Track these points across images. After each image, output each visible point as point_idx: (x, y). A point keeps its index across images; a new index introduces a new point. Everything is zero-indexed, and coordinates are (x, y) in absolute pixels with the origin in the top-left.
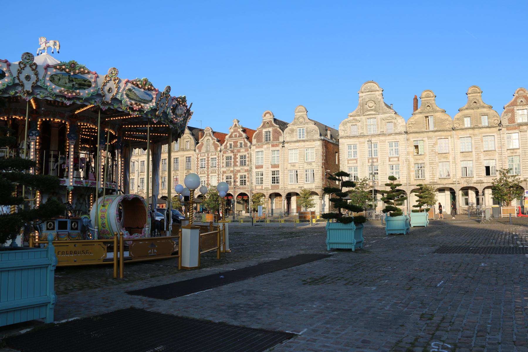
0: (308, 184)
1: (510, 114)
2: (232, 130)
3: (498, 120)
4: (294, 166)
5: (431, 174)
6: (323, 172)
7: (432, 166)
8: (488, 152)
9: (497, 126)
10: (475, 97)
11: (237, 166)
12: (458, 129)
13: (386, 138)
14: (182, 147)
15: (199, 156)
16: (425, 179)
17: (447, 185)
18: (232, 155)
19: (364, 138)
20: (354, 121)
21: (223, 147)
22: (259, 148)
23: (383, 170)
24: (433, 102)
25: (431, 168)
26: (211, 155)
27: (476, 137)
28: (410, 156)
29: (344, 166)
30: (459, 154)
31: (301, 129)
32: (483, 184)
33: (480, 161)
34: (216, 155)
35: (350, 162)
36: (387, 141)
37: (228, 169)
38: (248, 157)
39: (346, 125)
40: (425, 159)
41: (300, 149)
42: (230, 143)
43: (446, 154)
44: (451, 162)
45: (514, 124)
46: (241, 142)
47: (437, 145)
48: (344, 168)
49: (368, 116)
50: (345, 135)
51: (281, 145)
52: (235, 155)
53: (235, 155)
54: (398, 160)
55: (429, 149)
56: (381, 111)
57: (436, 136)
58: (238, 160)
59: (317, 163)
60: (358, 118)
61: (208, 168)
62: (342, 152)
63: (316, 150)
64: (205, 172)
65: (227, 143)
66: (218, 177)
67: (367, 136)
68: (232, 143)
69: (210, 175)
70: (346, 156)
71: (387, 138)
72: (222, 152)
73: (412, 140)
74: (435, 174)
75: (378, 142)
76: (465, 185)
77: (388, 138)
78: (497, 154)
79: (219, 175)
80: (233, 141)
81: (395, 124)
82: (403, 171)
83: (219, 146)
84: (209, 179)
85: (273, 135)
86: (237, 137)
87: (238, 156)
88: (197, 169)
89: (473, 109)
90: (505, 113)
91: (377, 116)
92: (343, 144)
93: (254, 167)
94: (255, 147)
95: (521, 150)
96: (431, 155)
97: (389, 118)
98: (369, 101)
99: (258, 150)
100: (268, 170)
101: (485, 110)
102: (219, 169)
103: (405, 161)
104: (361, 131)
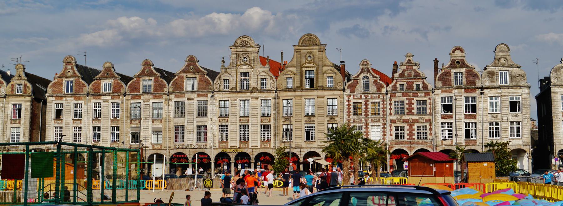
0: (519, 139)
2: (404, 67)
4: (496, 117)
11: (413, 114)
14: (320, 85)
15: (351, 98)
18: (404, 99)
21: (390, 88)
22: (445, 92)
26: (371, 98)
31: (503, 72)
34: (379, 98)
37: (399, 117)
38: (430, 104)
39: (559, 72)
41: (504, 97)
42: (402, 83)
46: (418, 83)
48: (558, 122)
50: (558, 83)
51: (479, 91)
52: (410, 100)
53: (410, 100)
58: (415, 106)
61: (366, 115)
62: (555, 103)
64: (361, 120)
65: (396, 83)
66: (384, 128)
68: (405, 83)
69: (370, 124)
72: (389, 95)
79: (384, 124)
80: (407, 81)
83: (383, 87)
84: (368, 130)
85: (466, 77)
86: (411, 77)
87: (414, 101)
88: (349, 115)
92: (556, 93)
93: (440, 117)
94: (440, 91)
99: (444, 95)
100: (460, 121)
102: (384, 117)
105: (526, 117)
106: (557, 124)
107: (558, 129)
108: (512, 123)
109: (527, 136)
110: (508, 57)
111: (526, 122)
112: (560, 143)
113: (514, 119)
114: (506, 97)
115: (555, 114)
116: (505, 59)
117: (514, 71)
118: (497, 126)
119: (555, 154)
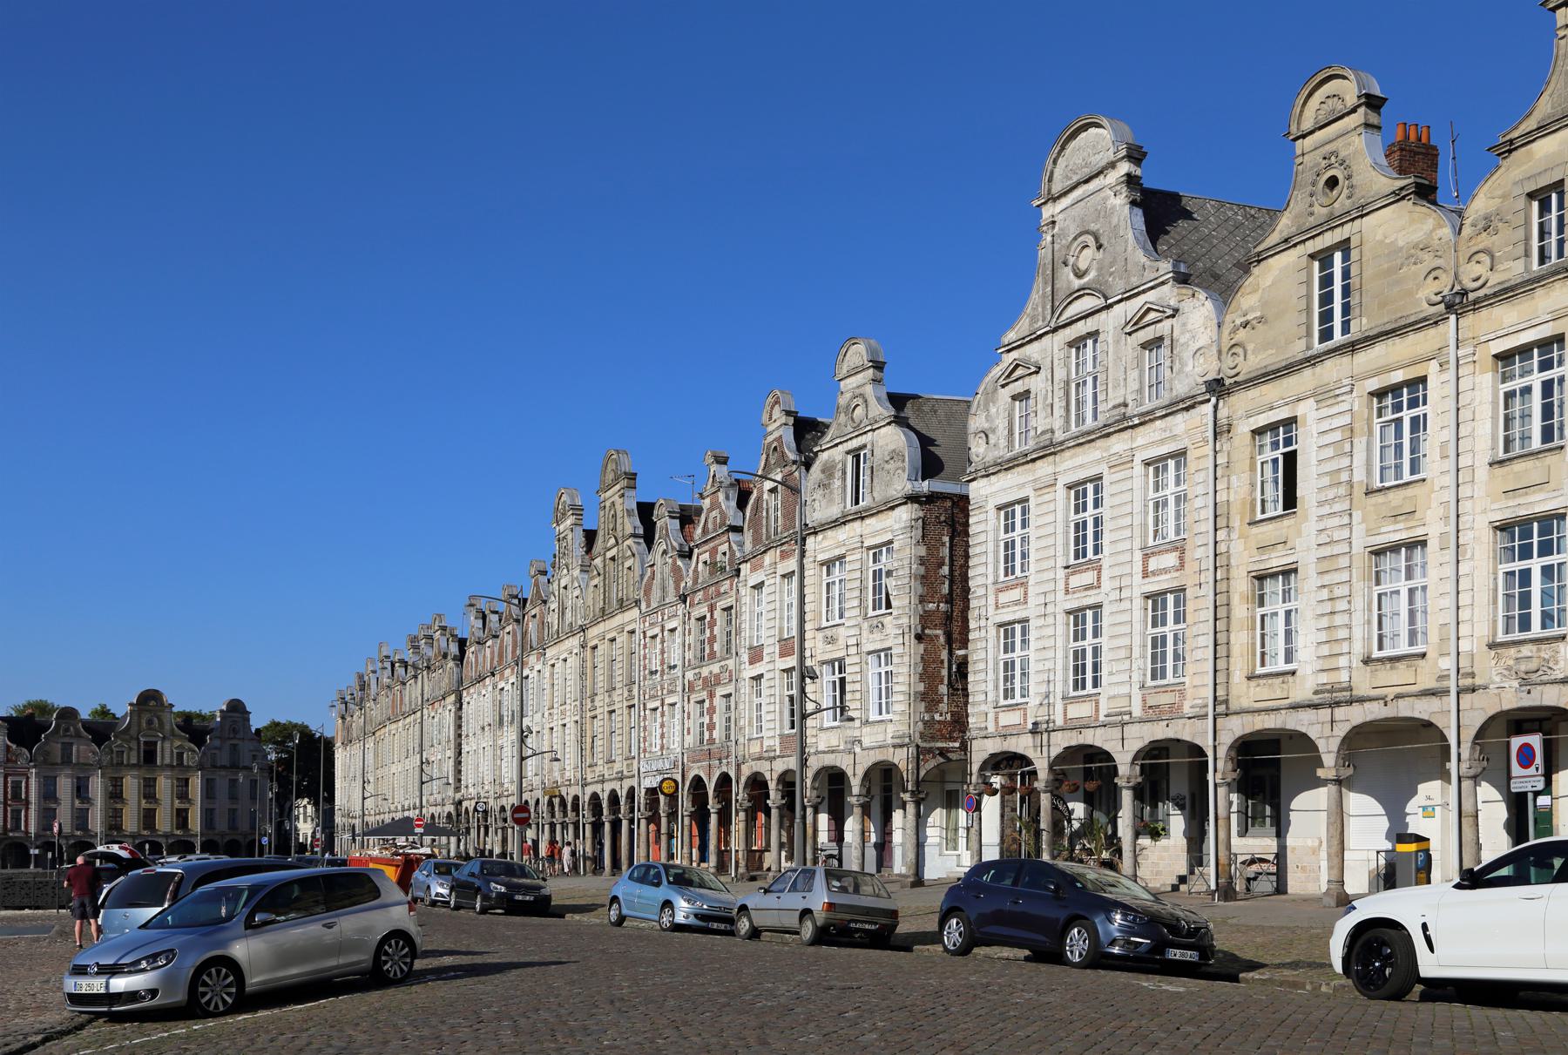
19: (1051, 458)
25: (1325, 594)
28: (1234, 536)
30: (1482, 472)
40: (1298, 543)
43: (1409, 491)
44: (1433, 544)
71: (1140, 441)
73: (1243, 428)
74: (1342, 633)
77: (1144, 436)
97: (1152, 316)
112: (980, 729)
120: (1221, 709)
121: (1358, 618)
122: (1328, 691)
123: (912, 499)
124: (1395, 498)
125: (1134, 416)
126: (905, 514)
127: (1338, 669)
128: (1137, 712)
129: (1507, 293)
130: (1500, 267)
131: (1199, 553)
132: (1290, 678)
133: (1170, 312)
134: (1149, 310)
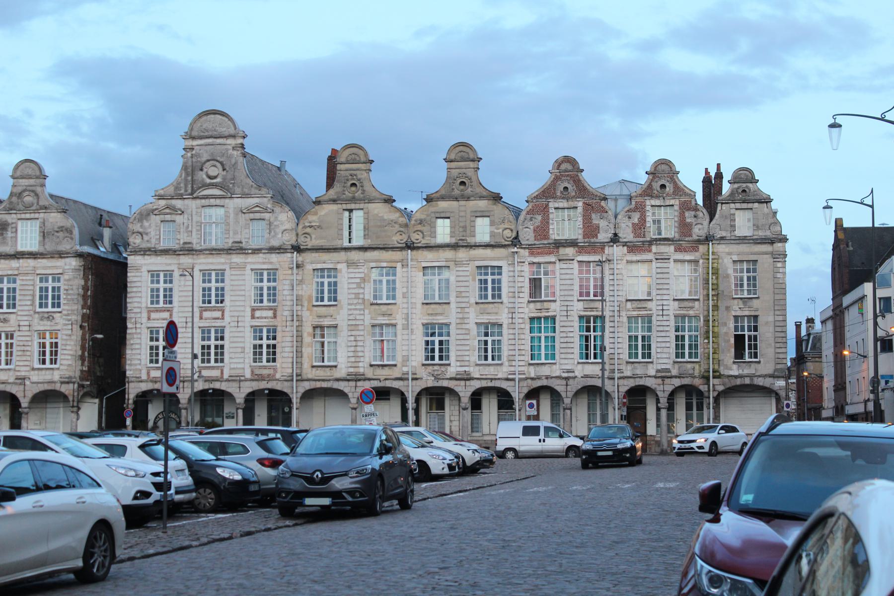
1: (539, 218)
3: (512, 230)
5: (351, 354)
6: (83, 339)
7: (354, 333)
8: (486, 306)
9: (508, 245)
10: (464, 171)
12: (419, 245)
13: (246, 259)
16: (336, 367)
17: (387, 382)
19: (190, 256)
20: (167, 211)
23: (235, 340)
24: (365, 174)
25: (352, 338)
27: (461, 269)
28: (305, 309)
29: (138, 326)
30: (419, 306)
32: (473, 383)
33: (467, 326)
35: (153, 315)
36: (249, 267)
39: (147, 220)
40: (338, 317)
41: (24, 278)
43: (390, 307)
44: (399, 327)
45: (546, 242)
47: (369, 282)
48: (138, 331)
49: (203, 201)
50: (144, 245)
54: (275, 317)
55: (350, 291)
56: (238, 190)
57: (366, 261)
59: (68, 315)
60: (178, 203)
62: (135, 290)
63: (65, 280)
67: (201, 251)
70: (144, 300)
74: (360, 354)
75: (227, 267)
76: (431, 383)
77: (251, 259)
78: (506, 310)
81: (270, 224)
82: (283, 344)
89: (456, 199)
90: (528, 213)
91: (227, 201)
92: (138, 269)
95: (558, 303)
96: (353, 307)
97: (257, 209)
98: (208, 161)
101: (483, 204)
103: (289, 318)
104: (183, 238)
105: (69, 320)
106: (135, 336)
107: (137, 346)
108: (42, 335)
109: (70, 363)
110: (39, 189)
111: (70, 332)
112: (138, 378)
113: (44, 325)
114: (28, 278)
115: (133, 315)
116: (32, 194)
117: (51, 220)
118: (9, 341)
119: (126, 401)
120: (299, 378)
121: (367, 349)
122: (354, 375)
123: (80, 255)
124: (384, 308)
125: (250, 249)
126: (74, 263)
127: (358, 367)
128: (248, 375)
129: (428, 247)
130: (427, 238)
131: (286, 313)
132: (334, 369)
133: (269, 211)
134: (257, 206)
